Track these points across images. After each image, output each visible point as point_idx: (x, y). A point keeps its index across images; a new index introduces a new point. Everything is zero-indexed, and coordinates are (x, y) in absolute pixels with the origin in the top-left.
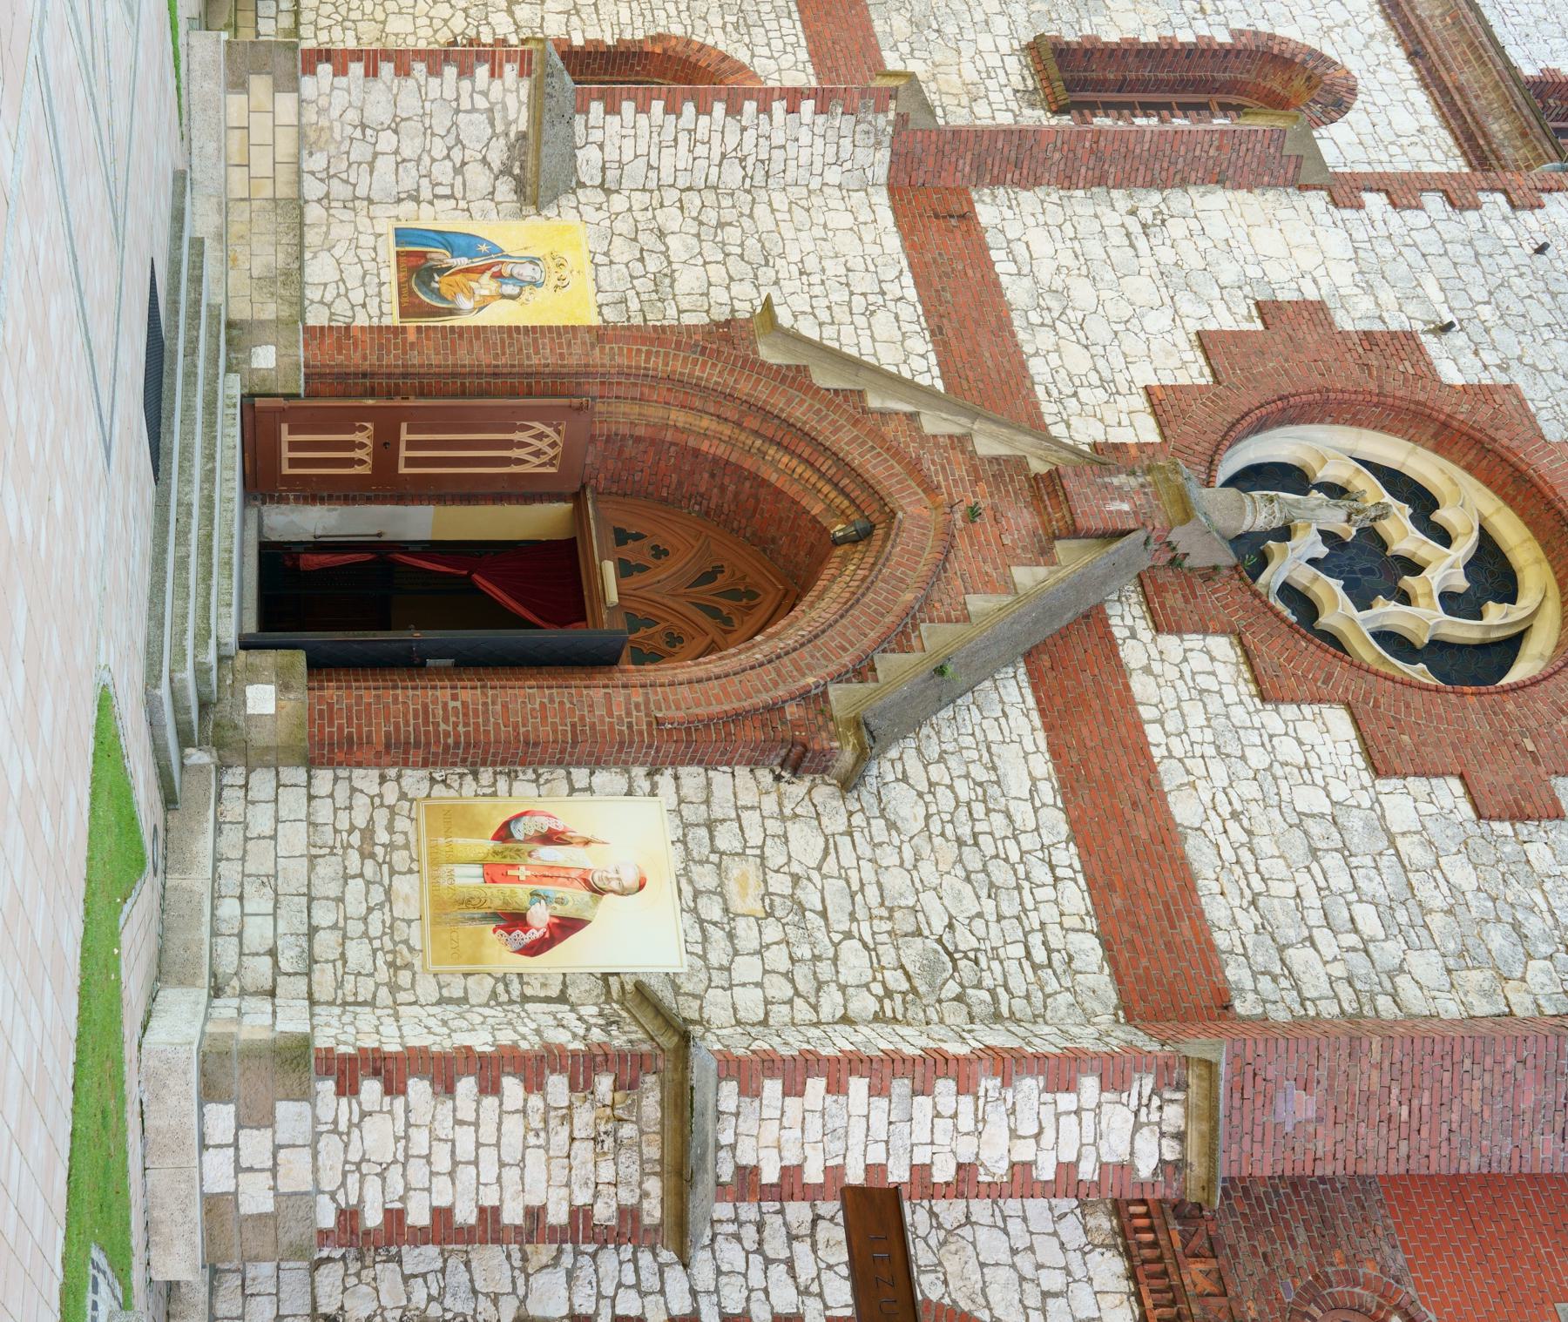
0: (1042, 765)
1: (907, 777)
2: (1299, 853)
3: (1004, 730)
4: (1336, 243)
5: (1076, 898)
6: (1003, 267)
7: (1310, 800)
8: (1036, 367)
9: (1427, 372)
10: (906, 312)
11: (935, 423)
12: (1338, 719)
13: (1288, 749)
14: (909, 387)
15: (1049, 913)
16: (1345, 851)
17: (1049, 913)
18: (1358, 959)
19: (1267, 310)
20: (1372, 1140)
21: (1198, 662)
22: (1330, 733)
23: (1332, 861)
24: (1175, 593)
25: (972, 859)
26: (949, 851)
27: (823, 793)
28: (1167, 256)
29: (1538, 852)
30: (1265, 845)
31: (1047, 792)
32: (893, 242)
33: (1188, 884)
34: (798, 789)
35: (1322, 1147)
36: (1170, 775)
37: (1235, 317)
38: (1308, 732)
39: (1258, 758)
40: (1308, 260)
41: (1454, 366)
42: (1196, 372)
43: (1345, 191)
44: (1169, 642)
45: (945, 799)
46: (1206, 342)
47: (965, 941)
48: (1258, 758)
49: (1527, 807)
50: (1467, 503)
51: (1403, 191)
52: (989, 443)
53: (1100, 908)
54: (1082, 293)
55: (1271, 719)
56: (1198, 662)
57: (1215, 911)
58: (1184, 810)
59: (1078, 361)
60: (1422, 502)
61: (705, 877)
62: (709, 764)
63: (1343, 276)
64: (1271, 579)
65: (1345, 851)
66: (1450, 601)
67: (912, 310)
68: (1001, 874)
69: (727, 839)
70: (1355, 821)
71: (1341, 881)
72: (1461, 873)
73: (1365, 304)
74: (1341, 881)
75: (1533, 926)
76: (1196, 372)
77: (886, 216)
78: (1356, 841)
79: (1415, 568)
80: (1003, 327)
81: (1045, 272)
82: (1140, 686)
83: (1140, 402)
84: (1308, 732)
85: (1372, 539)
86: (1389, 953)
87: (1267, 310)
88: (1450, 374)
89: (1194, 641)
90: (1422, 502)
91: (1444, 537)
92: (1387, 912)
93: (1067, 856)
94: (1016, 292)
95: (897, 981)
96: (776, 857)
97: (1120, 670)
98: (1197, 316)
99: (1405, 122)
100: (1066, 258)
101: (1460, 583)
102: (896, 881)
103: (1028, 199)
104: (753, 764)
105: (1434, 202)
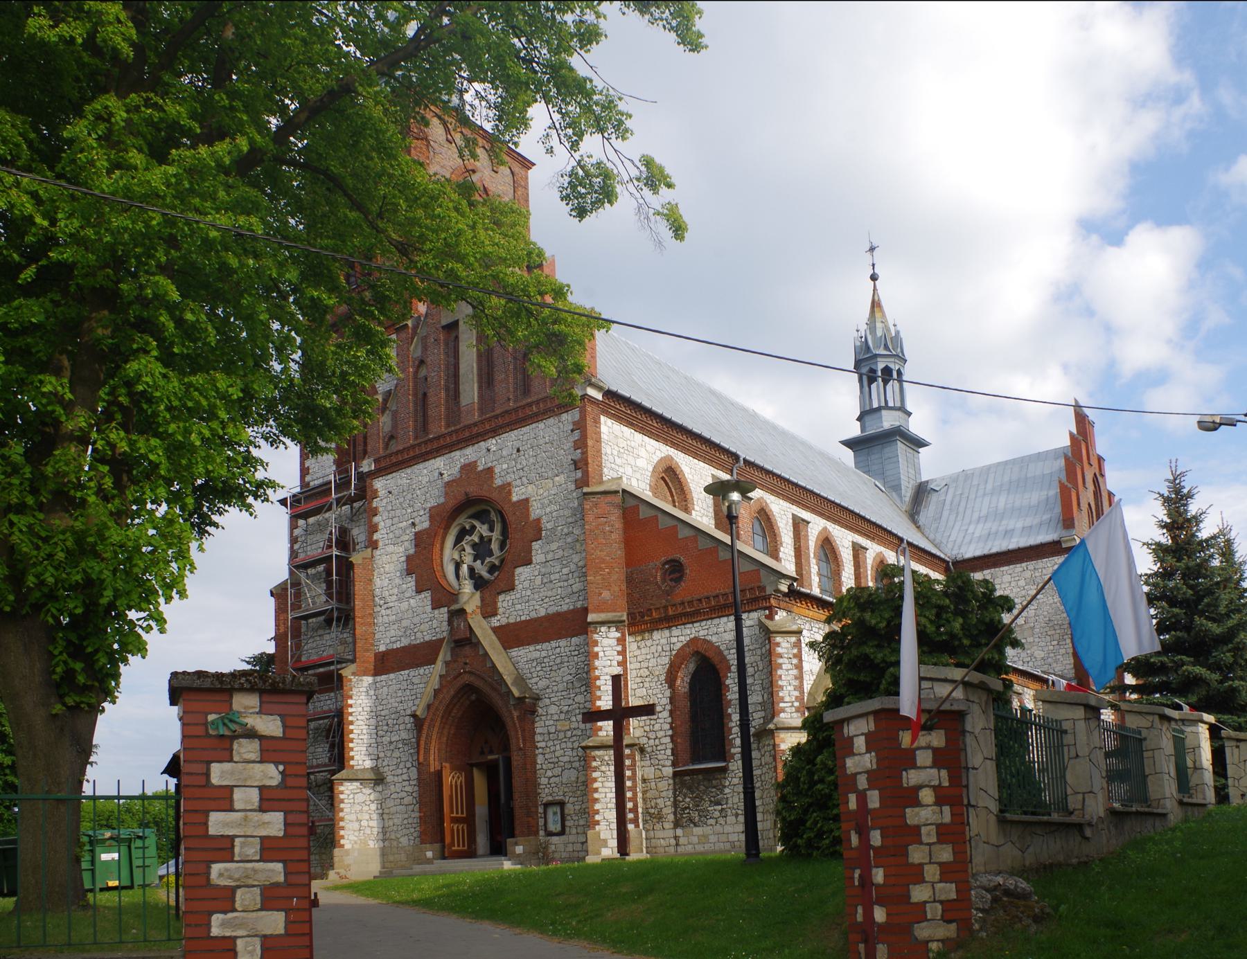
0: (532, 648)
1: (538, 684)
2: (551, 586)
4: (390, 548)
5: (563, 643)
6: (398, 645)
7: (538, 580)
8: (427, 638)
10: (412, 674)
13: (526, 584)
15: (567, 649)
16: (550, 574)
17: (567, 649)
18: (576, 574)
19: (409, 572)
20: (615, 577)
21: (505, 604)
23: (553, 577)
25: (555, 668)
26: (553, 674)
27: (541, 704)
28: (394, 598)
29: (549, 526)
30: (549, 594)
31: (538, 647)
33: (558, 614)
34: (540, 710)
35: (617, 589)
36: (533, 615)
37: (411, 582)
38: (522, 578)
39: (529, 593)
45: (541, 673)
47: (573, 671)
48: (529, 593)
53: (565, 637)
54: (405, 623)
56: (505, 604)
57: (565, 608)
58: (542, 613)
61: (561, 735)
62: (535, 733)
65: (550, 574)
66: (491, 530)
67: (413, 672)
68: (558, 661)
69: (552, 730)
70: (543, 570)
71: (557, 576)
72: (554, 546)
74: (557, 576)
75: (566, 530)
78: (548, 570)
80: (415, 646)
83: (436, 612)
84: (522, 578)
86: (573, 567)
87: (409, 572)
89: (499, 604)
93: (553, 644)
94: (405, 642)
95: (583, 689)
96: (556, 717)
100: (395, 627)
102: (561, 687)
104: (534, 722)
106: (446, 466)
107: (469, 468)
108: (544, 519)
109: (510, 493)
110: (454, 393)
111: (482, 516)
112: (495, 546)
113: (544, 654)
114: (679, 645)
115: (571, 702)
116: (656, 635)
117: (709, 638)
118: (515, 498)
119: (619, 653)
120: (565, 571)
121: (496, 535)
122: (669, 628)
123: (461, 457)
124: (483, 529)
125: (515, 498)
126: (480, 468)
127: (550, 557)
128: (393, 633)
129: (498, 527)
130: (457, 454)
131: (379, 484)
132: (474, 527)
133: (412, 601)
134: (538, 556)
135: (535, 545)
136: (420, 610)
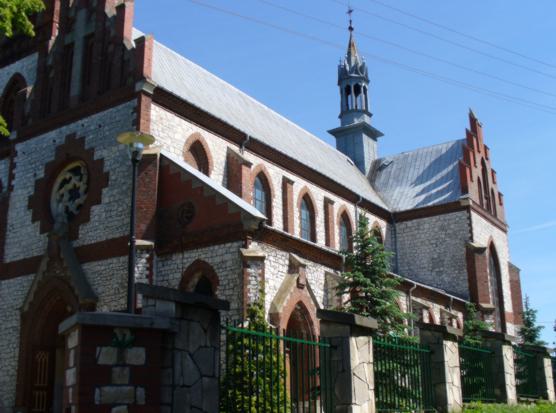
0: (95, 263)
2: (110, 219)
3: (93, 269)
4: (20, 192)
5: (115, 260)
6: (18, 259)
9: (42, 179)
11: (40, 277)
12: (93, 208)
14: (34, 281)
22: (96, 210)
23: (113, 213)
24: (73, 234)
29: (113, 178)
31: (100, 263)
32: (12, 280)
33: (113, 240)
36: (99, 240)
37: (29, 214)
40: (22, 197)
41: (41, 174)
42: (38, 223)
43: (11, 188)
44: (80, 236)
46: (33, 221)
49: (107, 176)
50: (65, 175)
51: (11, 177)
52: (43, 266)
54: (24, 243)
55: (92, 220)
57: (117, 235)
59: (34, 247)
60: (66, 181)
63: (25, 192)
64: (76, 212)
66: (81, 180)
73: (30, 189)
76: (38, 223)
77: (7, 281)
79: (75, 185)
81: (19, 250)
82: (85, 243)
85: (70, 191)
88: (42, 175)
90: (66, 181)
91: (70, 178)
92: (119, 206)
93: (109, 261)
94: (22, 257)
97: (84, 246)
98: (29, 222)
99: (3, 166)
101: (78, 178)
102: (112, 292)
103: (7, 252)
105: (14, 171)
106: (54, 137)
107: (71, 138)
108: (111, 173)
109: (93, 154)
110: (66, 85)
111: (76, 171)
112: (82, 190)
113: (103, 268)
114: (188, 264)
115: (115, 303)
116: (174, 257)
117: (206, 260)
118: (95, 158)
119: (148, 269)
120: (120, 209)
121: (82, 187)
122: (182, 252)
123: (66, 130)
124: (75, 180)
125: (95, 158)
126: (77, 137)
127: (112, 199)
128: (15, 250)
129: (85, 179)
130: (64, 128)
131: (19, 147)
132: (70, 178)
133: (29, 228)
134: (105, 200)
135: (105, 191)
136: (33, 234)
